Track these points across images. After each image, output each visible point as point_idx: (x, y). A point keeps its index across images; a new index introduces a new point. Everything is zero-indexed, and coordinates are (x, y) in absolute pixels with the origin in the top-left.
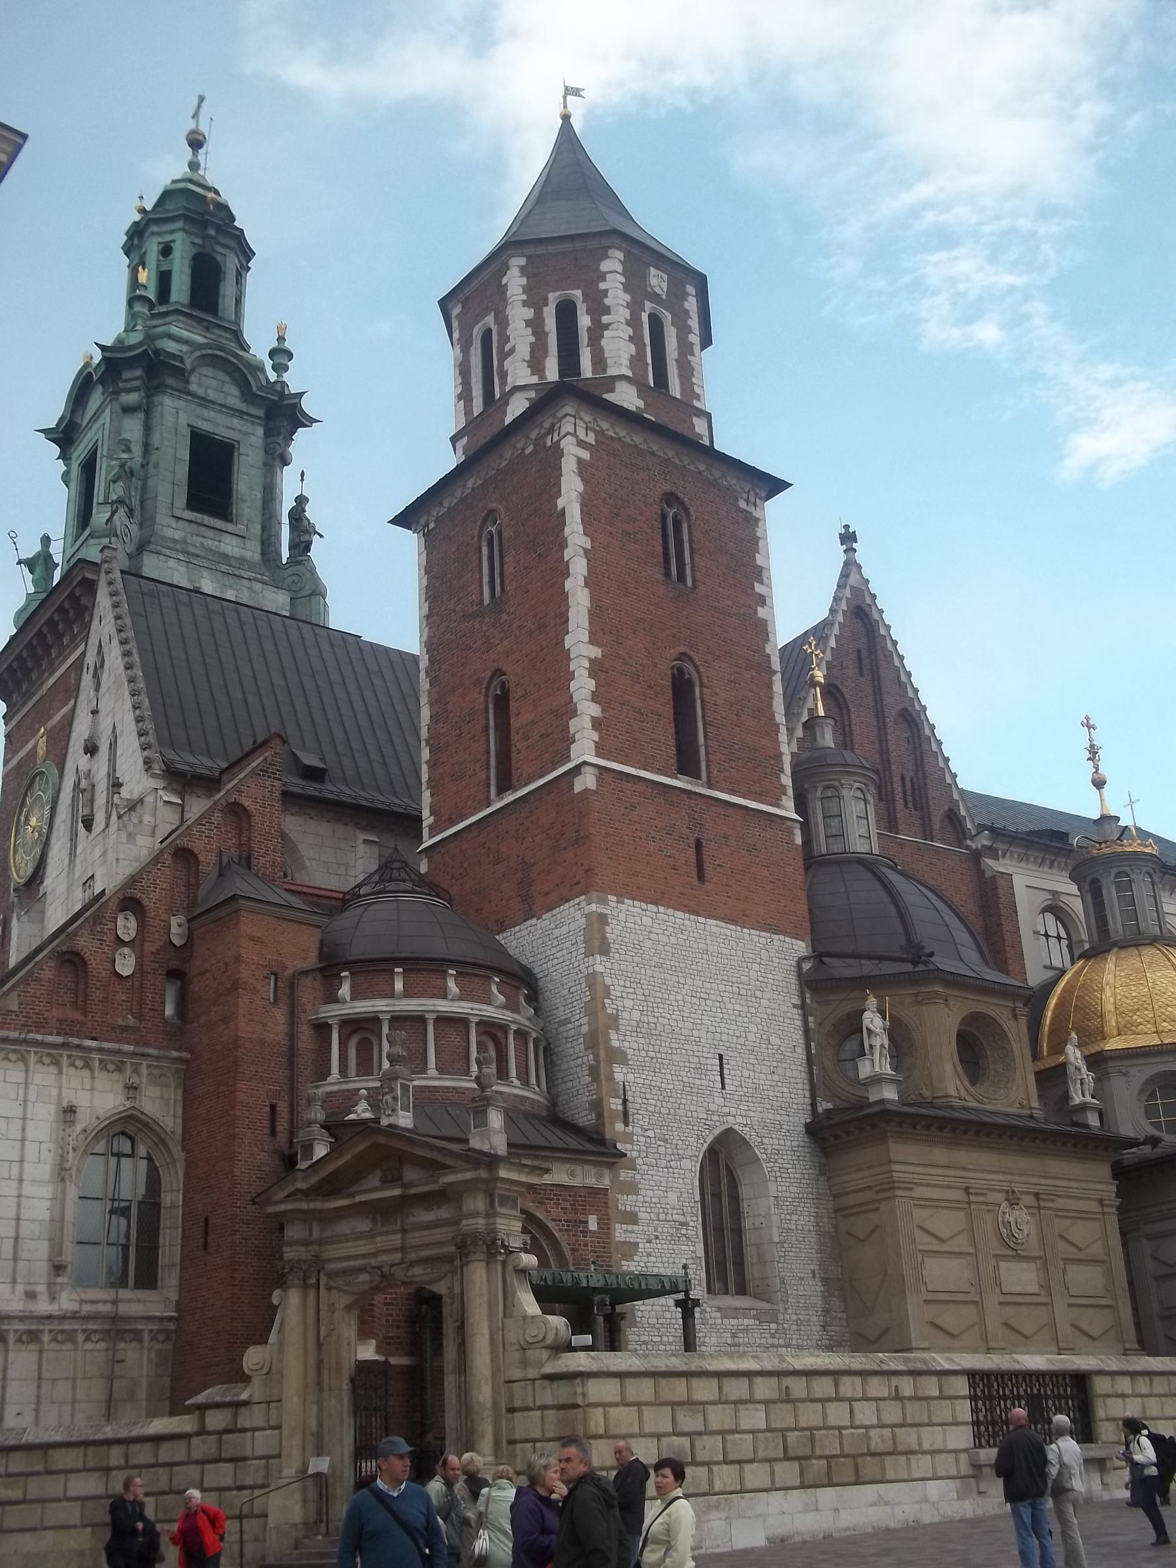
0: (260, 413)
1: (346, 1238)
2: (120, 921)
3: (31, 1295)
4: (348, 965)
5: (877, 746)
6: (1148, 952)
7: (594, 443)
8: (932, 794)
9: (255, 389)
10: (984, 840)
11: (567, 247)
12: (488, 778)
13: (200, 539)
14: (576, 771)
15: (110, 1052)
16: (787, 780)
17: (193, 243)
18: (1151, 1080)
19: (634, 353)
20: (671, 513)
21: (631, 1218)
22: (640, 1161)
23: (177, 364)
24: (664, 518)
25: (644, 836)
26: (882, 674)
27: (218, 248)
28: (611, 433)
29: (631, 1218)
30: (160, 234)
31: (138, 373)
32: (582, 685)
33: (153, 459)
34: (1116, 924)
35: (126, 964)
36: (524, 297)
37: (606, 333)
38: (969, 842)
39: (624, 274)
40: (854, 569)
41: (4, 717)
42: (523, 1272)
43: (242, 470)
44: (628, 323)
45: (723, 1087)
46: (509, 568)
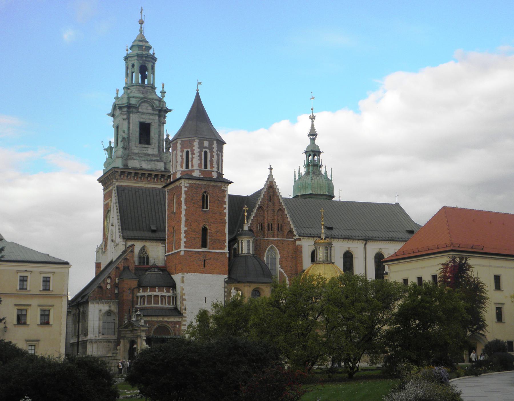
0: (157, 112)
1: (128, 333)
2: (108, 280)
3: (96, 337)
4: (141, 287)
5: (272, 218)
7: (188, 186)
8: (285, 227)
9: (155, 108)
10: (297, 237)
11: (188, 139)
12: (173, 246)
14: (180, 251)
15: (106, 301)
16: (227, 244)
17: (139, 63)
20: (205, 195)
22: (187, 316)
23: (135, 106)
24: (203, 196)
28: (192, 183)
30: (131, 61)
32: (183, 235)
33: (131, 131)
35: (109, 287)
36: (180, 150)
37: (194, 159)
40: (271, 177)
41: (103, 190)
42: (144, 340)
44: (198, 156)
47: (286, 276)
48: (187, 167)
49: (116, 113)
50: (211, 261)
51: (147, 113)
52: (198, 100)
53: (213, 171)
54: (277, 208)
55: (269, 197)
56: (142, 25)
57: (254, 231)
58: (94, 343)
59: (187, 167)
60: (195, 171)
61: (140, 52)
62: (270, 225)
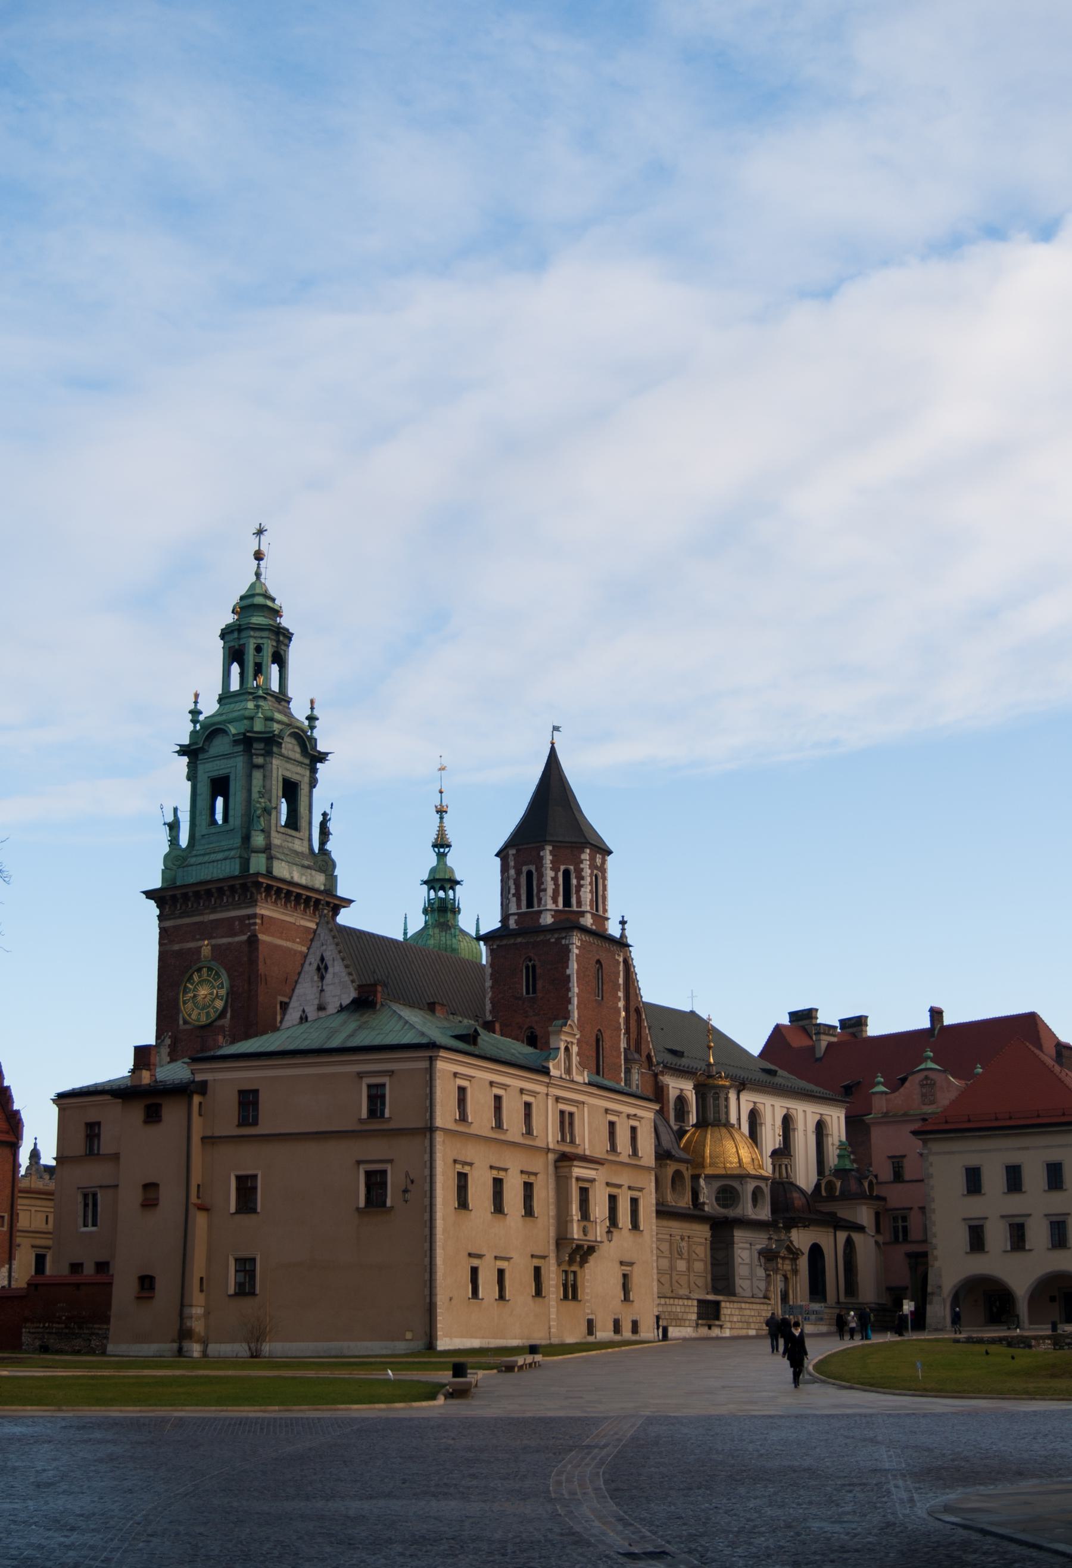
6: (724, 1130)
8: (643, 1047)
9: (309, 750)
11: (570, 845)
13: (286, 843)
16: (623, 1075)
23: (281, 741)
27: (283, 647)
30: (255, 637)
31: (262, 746)
34: (711, 1116)
36: (551, 866)
37: (582, 889)
38: (653, 1068)
43: (302, 799)
46: (540, 984)
48: (567, 902)
49: (209, 747)
51: (295, 760)
52: (553, 763)
56: (261, 562)
59: (567, 902)
60: (586, 914)
61: (271, 622)
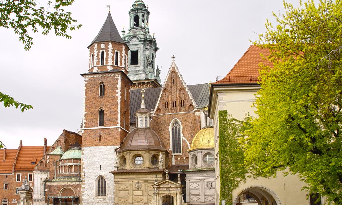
10: (196, 109)
11: (92, 46)
16: (119, 121)
18: (193, 156)
19: (97, 61)
20: (102, 85)
21: (84, 188)
25: (91, 137)
26: (177, 83)
27: (138, 13)
28: (92, 77)
29: (84, 188)
35: (48, 161)
37: (94, 59)
39: (97, 48)
40: (173, 64)
45: (100, 169)
47: (188, 143)
50: (105, 135)
51: (136, 44)
53: (108, 66)
54: (179, 88)
55: (173, 80)
57: (161, 109)
58: (37, 201)
62: (174, 102)
